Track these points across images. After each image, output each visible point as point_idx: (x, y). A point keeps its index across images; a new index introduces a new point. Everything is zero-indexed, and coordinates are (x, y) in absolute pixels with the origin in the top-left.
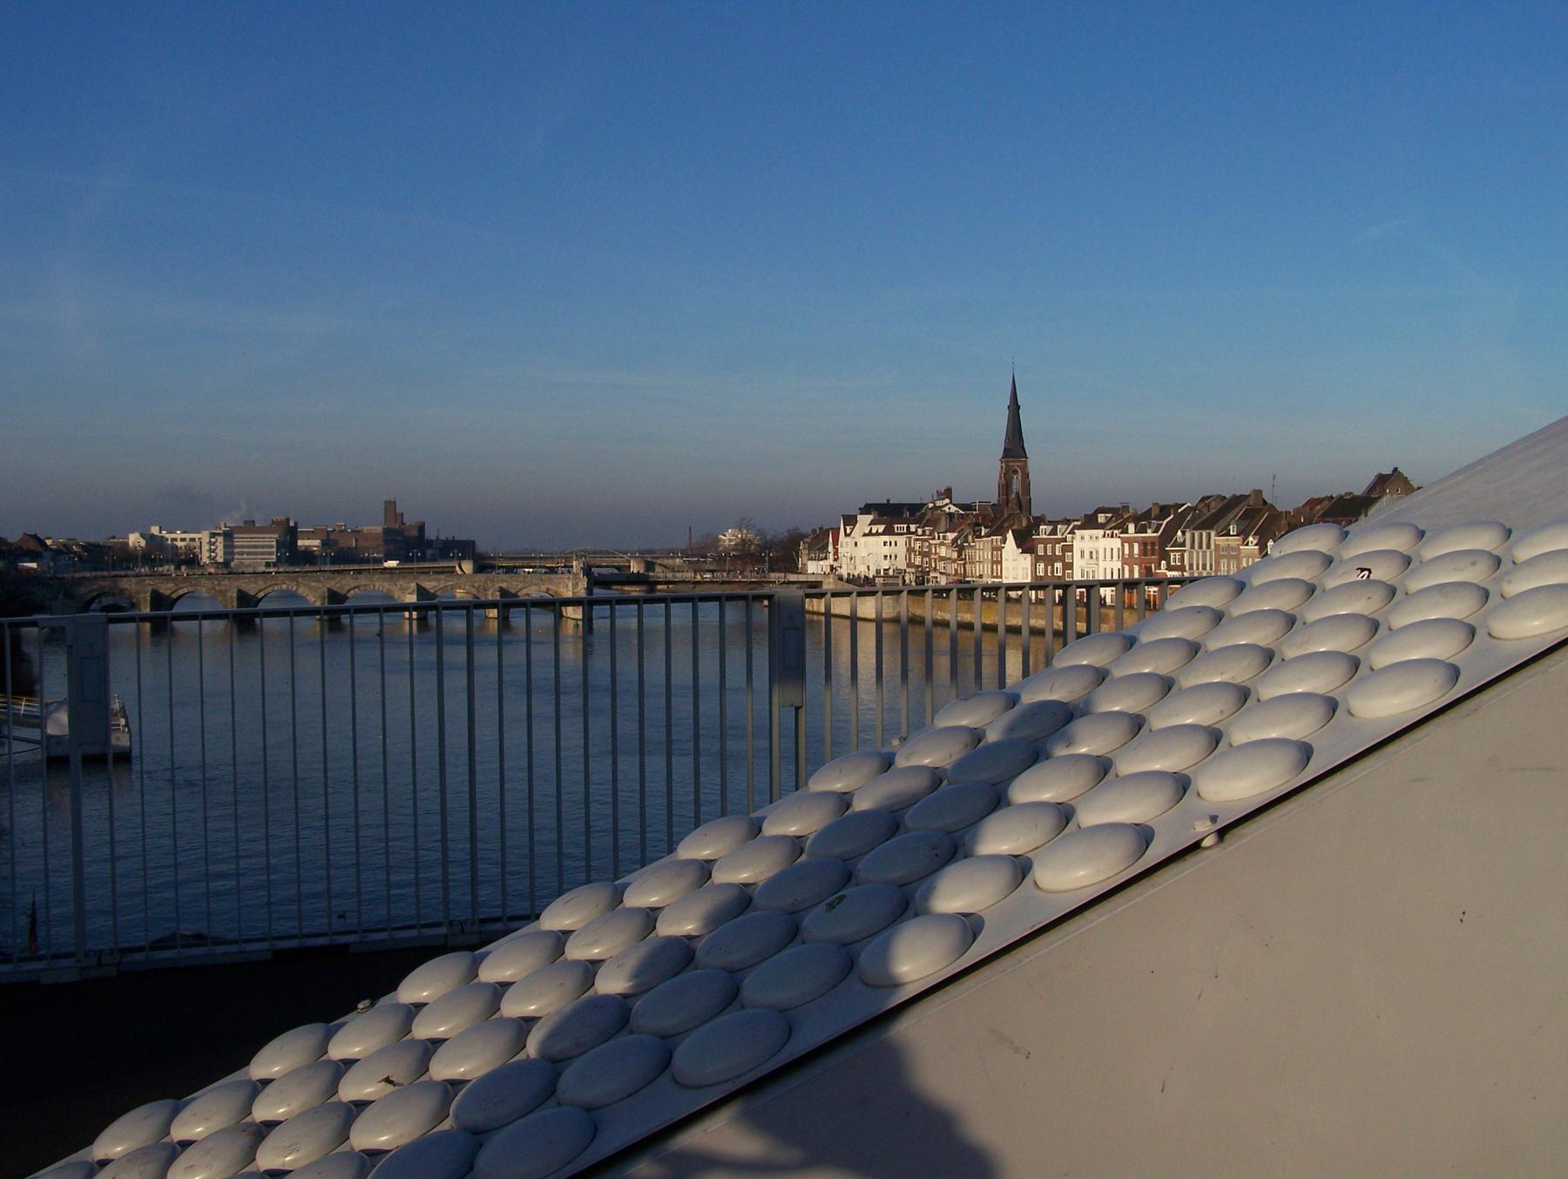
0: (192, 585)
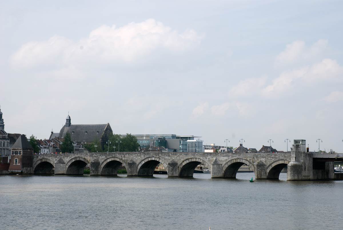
0: (113, 157)
